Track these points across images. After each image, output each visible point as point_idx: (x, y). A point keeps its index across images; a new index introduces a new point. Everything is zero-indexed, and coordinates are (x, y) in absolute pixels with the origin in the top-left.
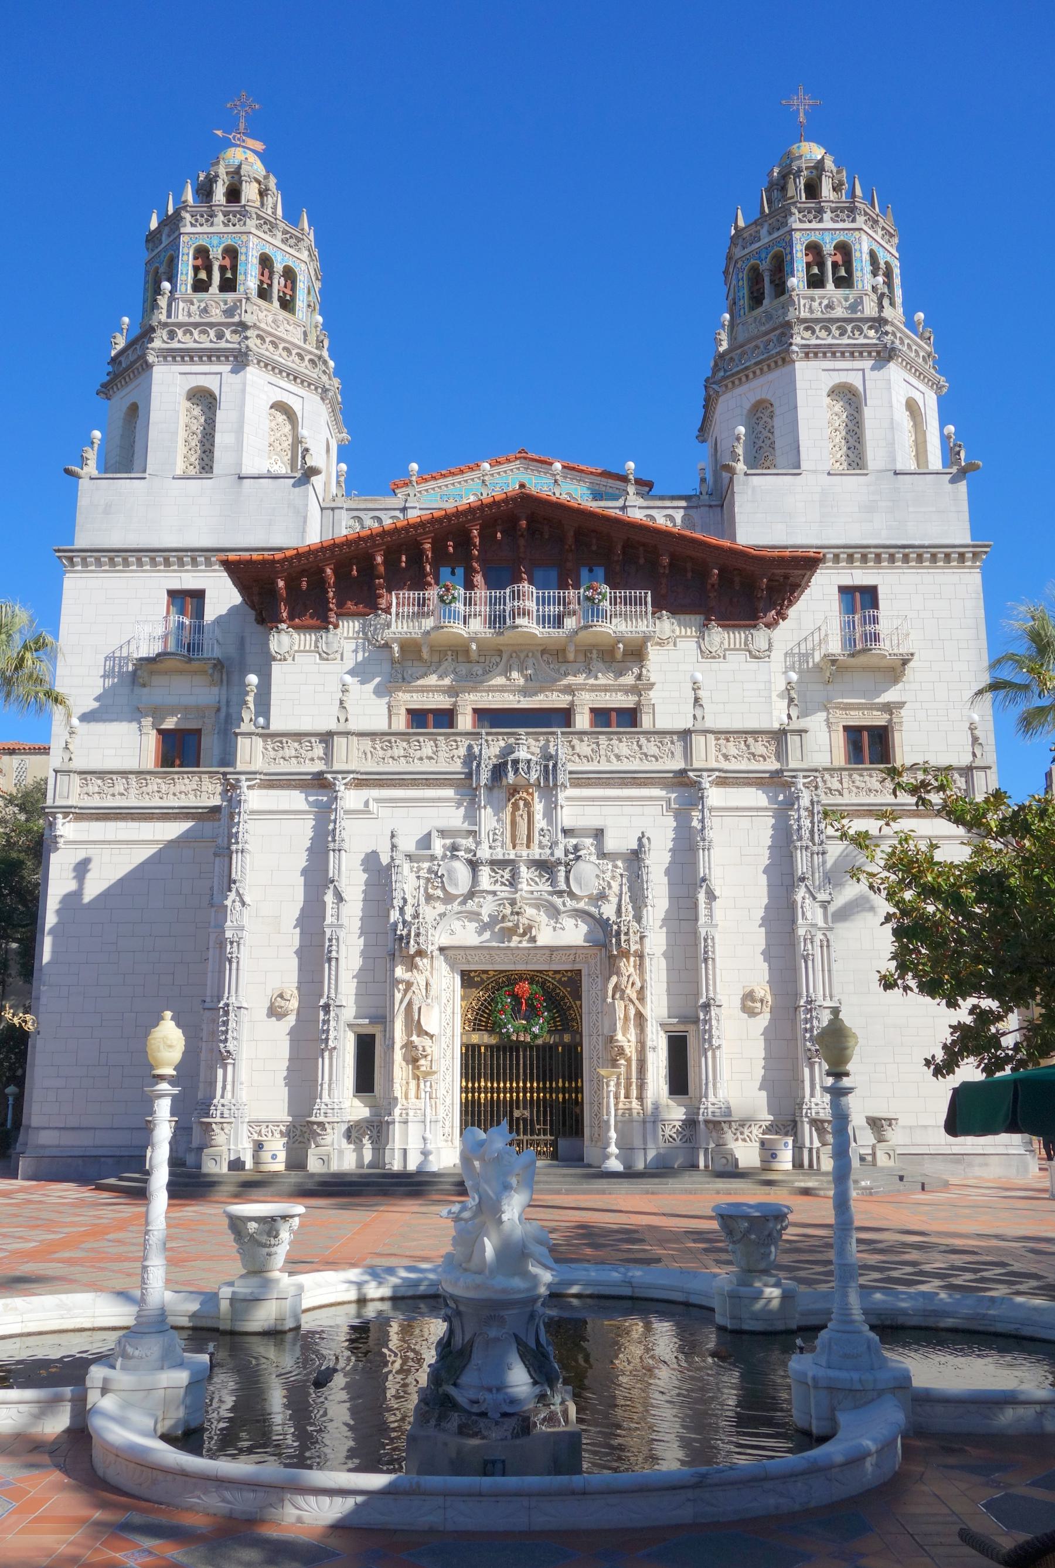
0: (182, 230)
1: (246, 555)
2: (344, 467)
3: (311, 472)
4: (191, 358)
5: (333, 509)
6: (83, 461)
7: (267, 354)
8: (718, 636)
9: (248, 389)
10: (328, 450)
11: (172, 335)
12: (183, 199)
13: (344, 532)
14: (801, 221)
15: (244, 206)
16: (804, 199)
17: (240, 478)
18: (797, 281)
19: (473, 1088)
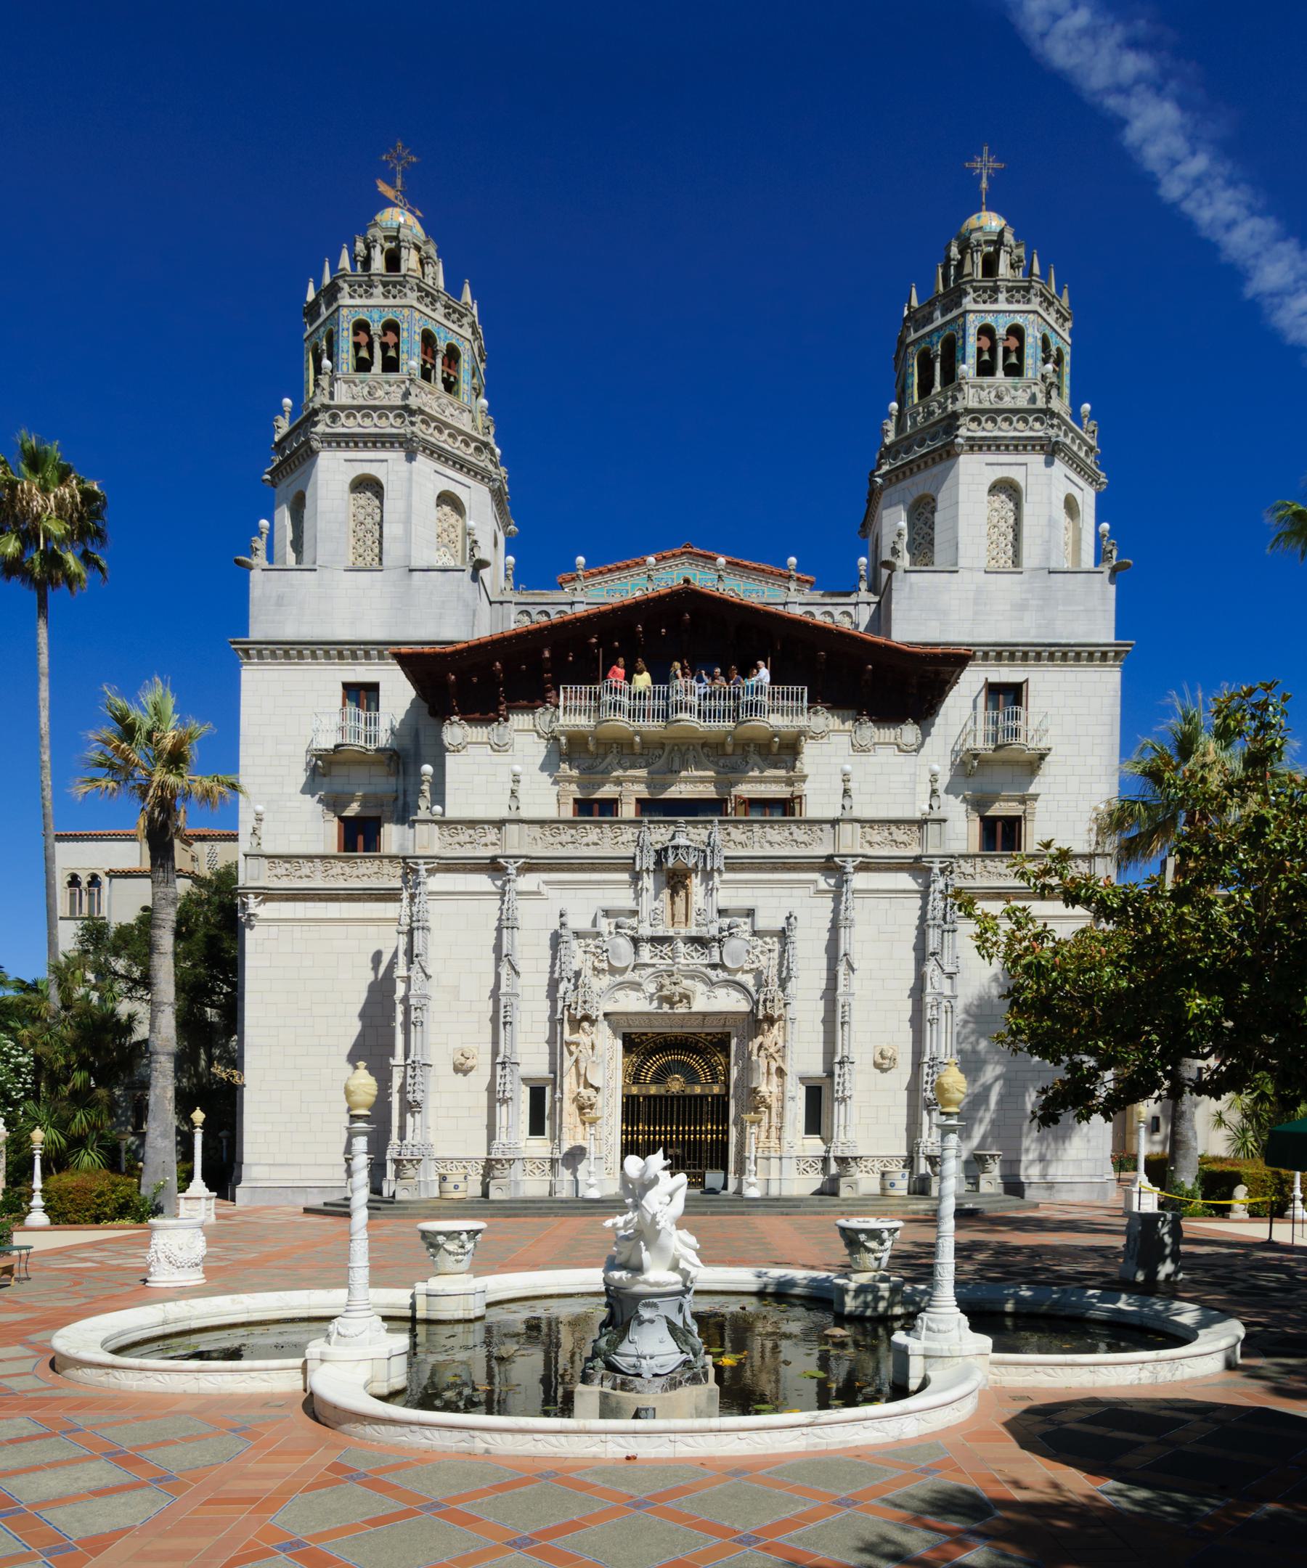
0: (341, 302)
1: (418, 648)
2: (511, 559)
3: (480, 565)
4: (356, 444)
5: (501, 603)
6: (252, 551)
7: (432, 440)
8: (870, 732)
9: (415, 477)
10: (496, 544)
11: (334, 418)
12: (340, 267)
13: (513, 626)
14: (976, 302)
15: (404, 276)
16: (980, 277)
17: (411, 570)
18: (967, 369)
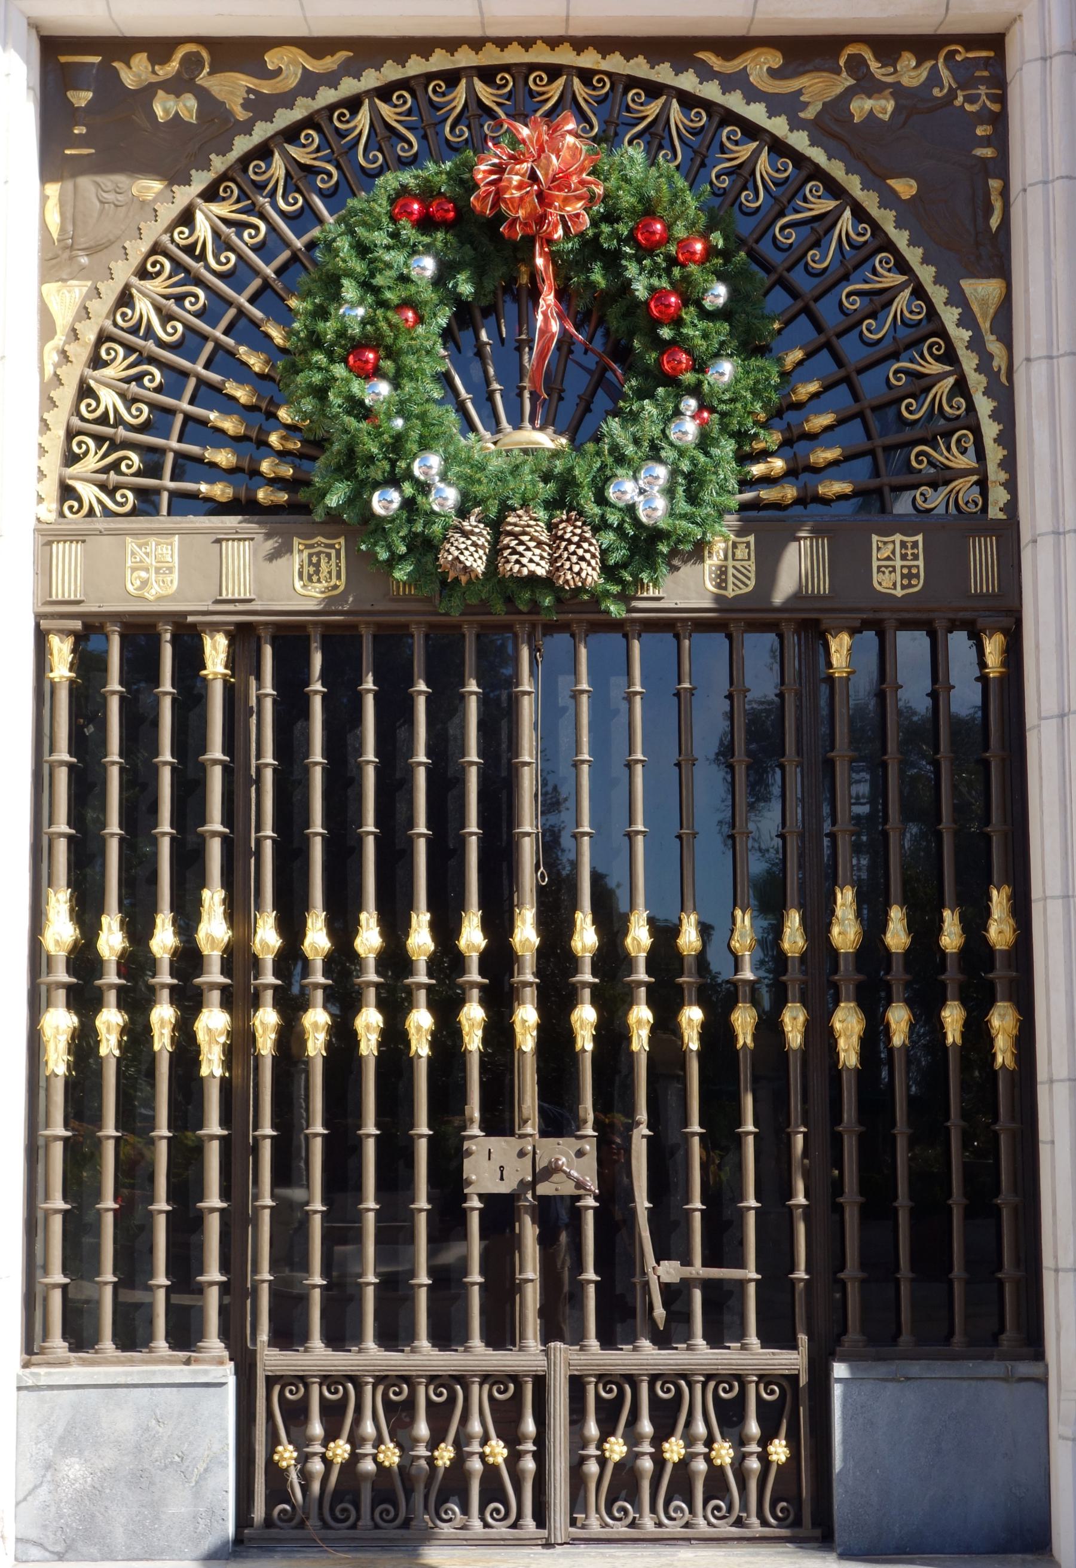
19: (137, 961)
